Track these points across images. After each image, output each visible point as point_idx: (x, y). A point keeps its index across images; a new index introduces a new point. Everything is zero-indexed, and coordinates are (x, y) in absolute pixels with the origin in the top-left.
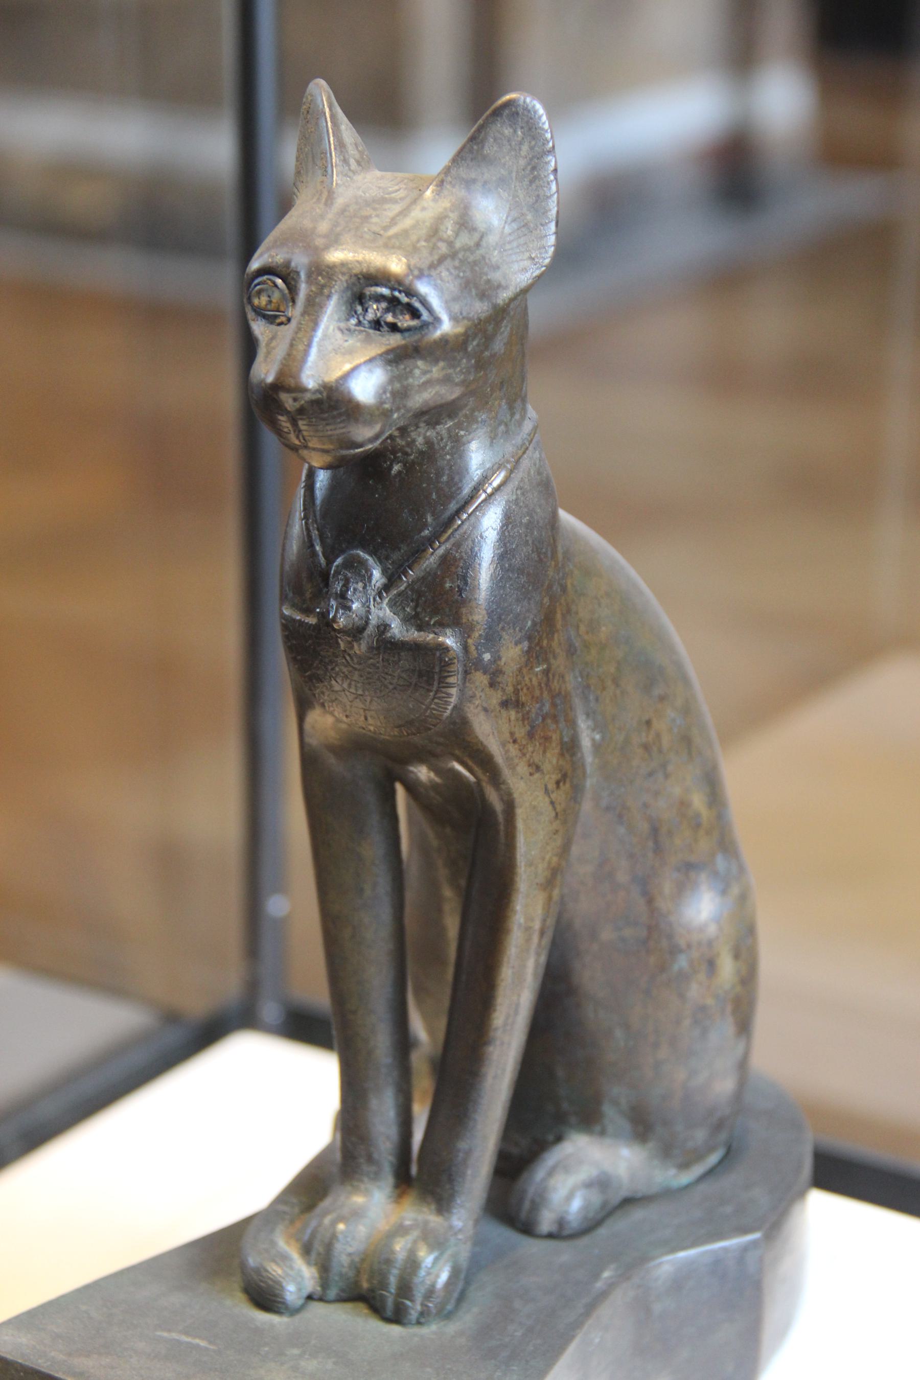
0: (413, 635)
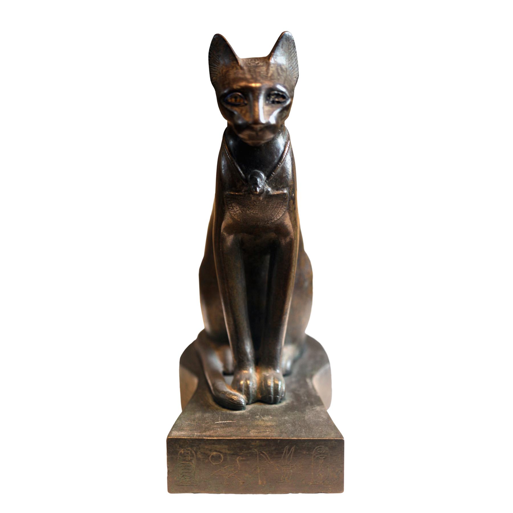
0: (276, 193)
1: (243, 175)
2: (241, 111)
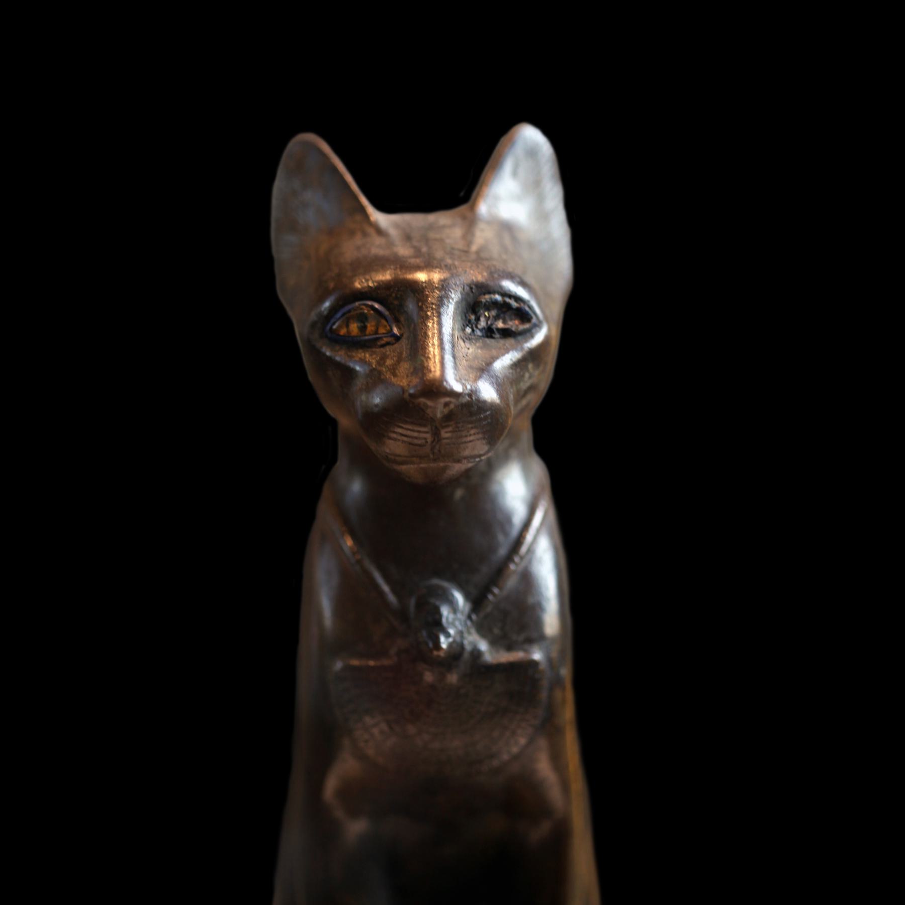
0: (505, 657)
1: (392, 598)
2: (383, 358)
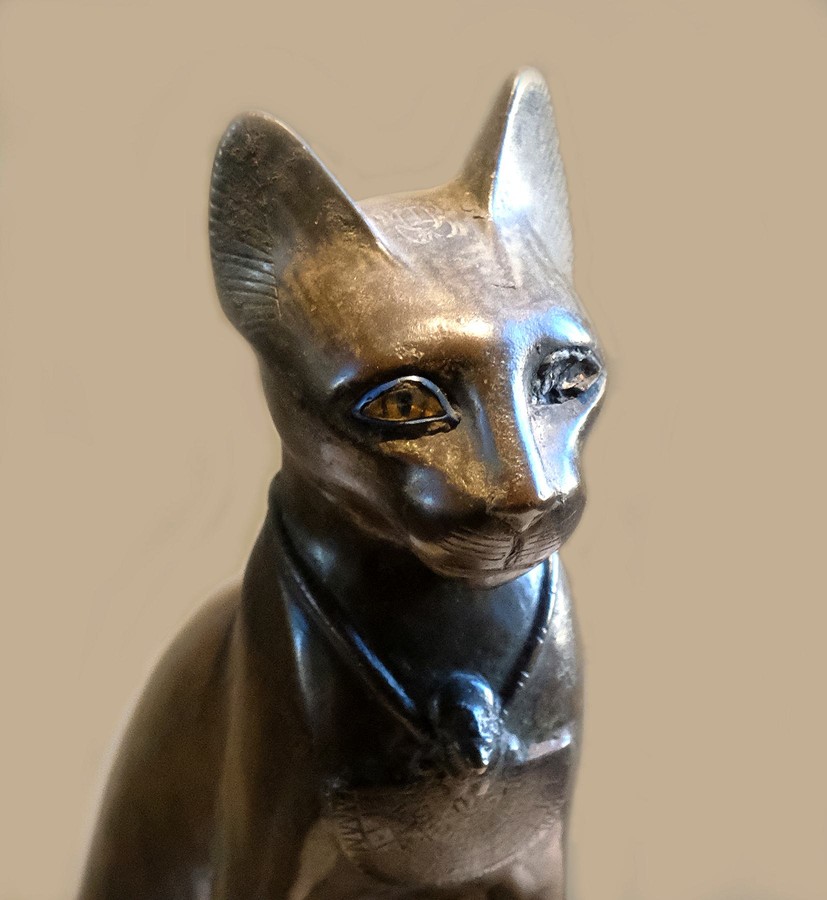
1: (408, 702)
